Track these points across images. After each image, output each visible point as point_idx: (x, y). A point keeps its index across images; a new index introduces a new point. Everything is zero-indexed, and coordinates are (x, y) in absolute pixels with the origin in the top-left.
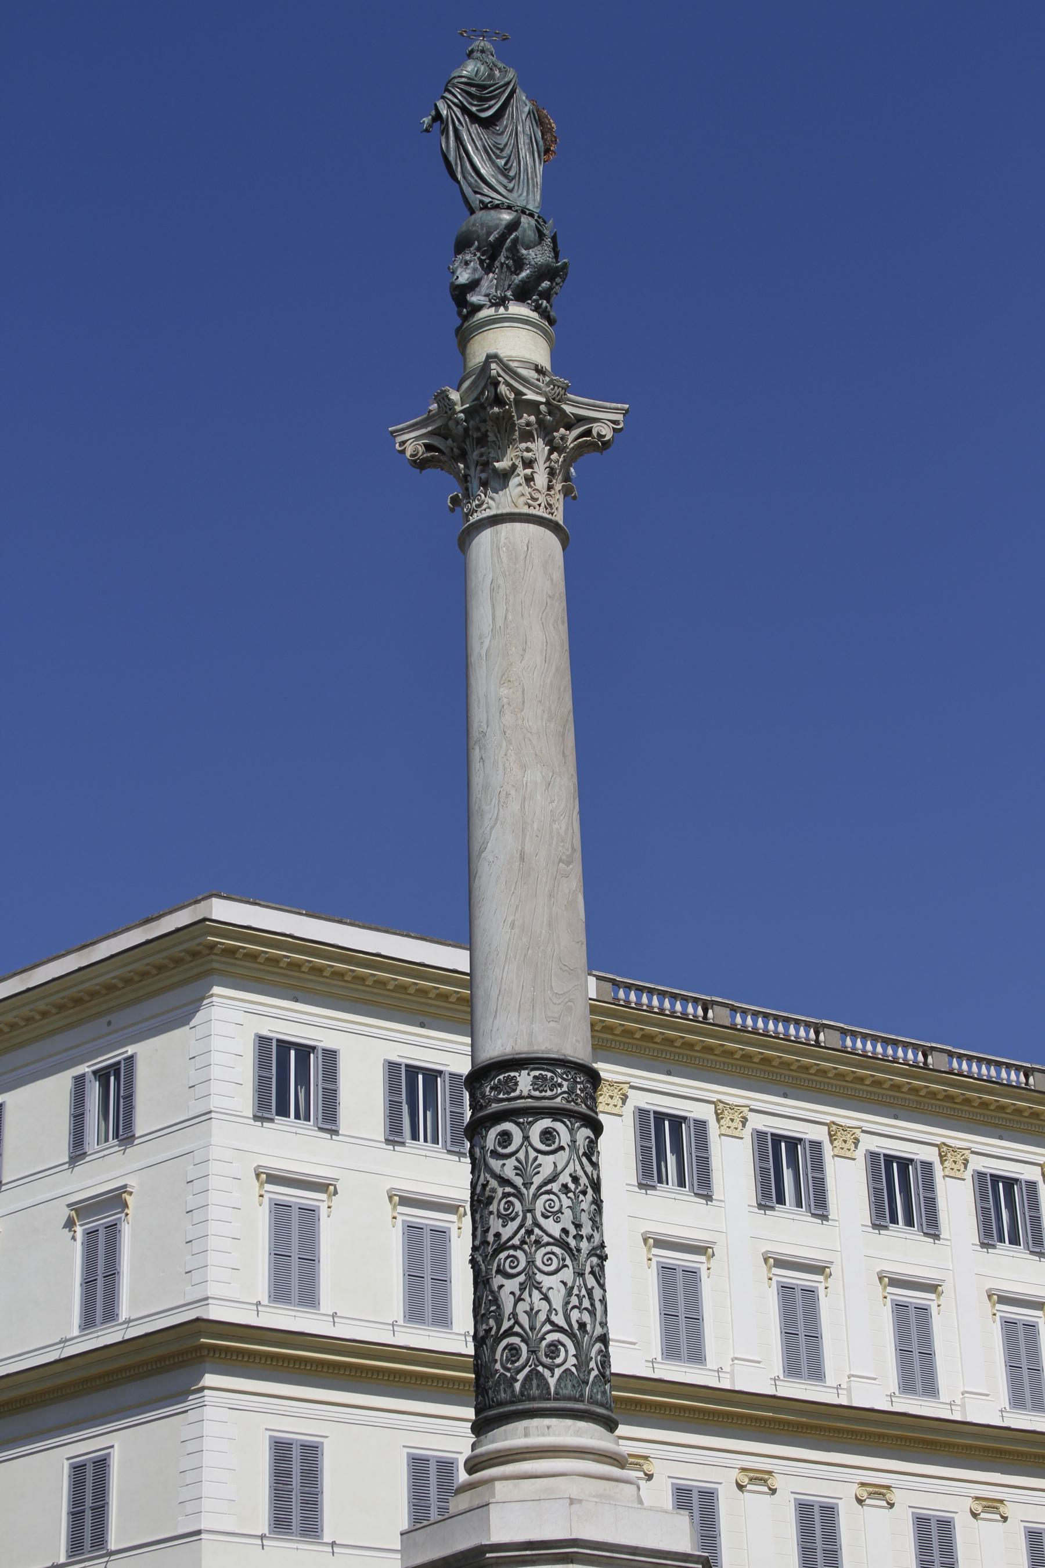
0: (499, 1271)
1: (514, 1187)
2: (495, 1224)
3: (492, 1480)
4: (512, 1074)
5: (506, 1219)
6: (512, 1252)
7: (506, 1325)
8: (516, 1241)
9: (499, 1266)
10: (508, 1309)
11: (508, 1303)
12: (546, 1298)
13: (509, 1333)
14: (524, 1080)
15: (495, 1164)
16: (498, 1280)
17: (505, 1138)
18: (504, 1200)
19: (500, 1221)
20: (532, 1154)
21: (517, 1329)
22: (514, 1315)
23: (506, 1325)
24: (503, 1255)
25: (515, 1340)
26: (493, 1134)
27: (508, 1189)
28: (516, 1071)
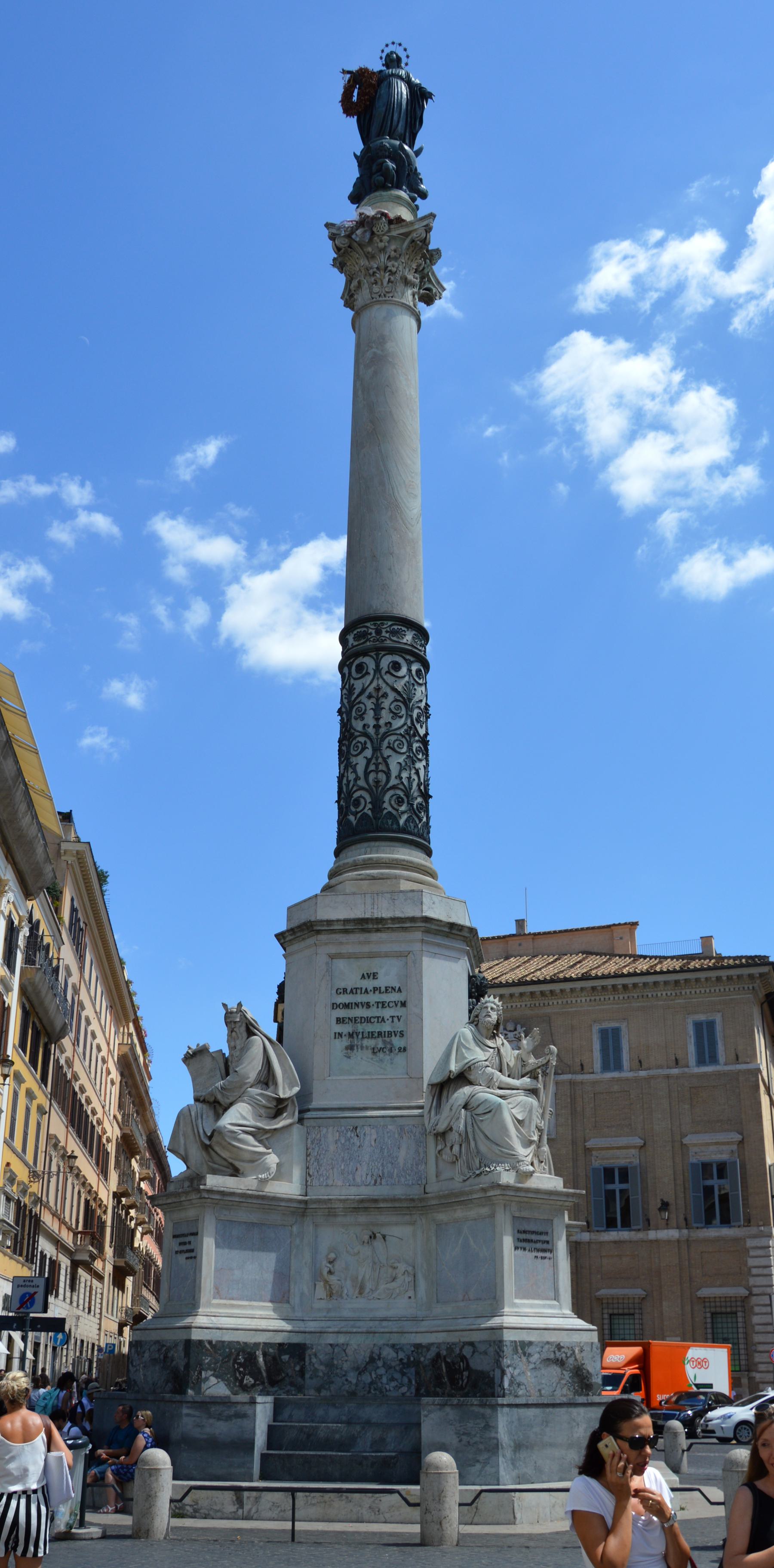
0: (389, 747)
1: (403, 698)
2: (386, 716)
3: (397, 877)
4: (403, 629)
5: (396, 715)
6: (400, 737)
7: (393, 781)
8: (402, 731)
9: (389, 743)
11: (394, 770)
12: (417, 773)
13: (394, 787)
15: (388, 678)
16: (387, 753)
17: (396, 666)
18: (395, 703)
19: (391, 715)
20: (412, 681)
21: (401, 786)
22: (399, 777)
23: (393, 781)
24: (392, 738)
25: (401, 794)
26: (386, 661)
27: (399, 698)
28: (408, 628)
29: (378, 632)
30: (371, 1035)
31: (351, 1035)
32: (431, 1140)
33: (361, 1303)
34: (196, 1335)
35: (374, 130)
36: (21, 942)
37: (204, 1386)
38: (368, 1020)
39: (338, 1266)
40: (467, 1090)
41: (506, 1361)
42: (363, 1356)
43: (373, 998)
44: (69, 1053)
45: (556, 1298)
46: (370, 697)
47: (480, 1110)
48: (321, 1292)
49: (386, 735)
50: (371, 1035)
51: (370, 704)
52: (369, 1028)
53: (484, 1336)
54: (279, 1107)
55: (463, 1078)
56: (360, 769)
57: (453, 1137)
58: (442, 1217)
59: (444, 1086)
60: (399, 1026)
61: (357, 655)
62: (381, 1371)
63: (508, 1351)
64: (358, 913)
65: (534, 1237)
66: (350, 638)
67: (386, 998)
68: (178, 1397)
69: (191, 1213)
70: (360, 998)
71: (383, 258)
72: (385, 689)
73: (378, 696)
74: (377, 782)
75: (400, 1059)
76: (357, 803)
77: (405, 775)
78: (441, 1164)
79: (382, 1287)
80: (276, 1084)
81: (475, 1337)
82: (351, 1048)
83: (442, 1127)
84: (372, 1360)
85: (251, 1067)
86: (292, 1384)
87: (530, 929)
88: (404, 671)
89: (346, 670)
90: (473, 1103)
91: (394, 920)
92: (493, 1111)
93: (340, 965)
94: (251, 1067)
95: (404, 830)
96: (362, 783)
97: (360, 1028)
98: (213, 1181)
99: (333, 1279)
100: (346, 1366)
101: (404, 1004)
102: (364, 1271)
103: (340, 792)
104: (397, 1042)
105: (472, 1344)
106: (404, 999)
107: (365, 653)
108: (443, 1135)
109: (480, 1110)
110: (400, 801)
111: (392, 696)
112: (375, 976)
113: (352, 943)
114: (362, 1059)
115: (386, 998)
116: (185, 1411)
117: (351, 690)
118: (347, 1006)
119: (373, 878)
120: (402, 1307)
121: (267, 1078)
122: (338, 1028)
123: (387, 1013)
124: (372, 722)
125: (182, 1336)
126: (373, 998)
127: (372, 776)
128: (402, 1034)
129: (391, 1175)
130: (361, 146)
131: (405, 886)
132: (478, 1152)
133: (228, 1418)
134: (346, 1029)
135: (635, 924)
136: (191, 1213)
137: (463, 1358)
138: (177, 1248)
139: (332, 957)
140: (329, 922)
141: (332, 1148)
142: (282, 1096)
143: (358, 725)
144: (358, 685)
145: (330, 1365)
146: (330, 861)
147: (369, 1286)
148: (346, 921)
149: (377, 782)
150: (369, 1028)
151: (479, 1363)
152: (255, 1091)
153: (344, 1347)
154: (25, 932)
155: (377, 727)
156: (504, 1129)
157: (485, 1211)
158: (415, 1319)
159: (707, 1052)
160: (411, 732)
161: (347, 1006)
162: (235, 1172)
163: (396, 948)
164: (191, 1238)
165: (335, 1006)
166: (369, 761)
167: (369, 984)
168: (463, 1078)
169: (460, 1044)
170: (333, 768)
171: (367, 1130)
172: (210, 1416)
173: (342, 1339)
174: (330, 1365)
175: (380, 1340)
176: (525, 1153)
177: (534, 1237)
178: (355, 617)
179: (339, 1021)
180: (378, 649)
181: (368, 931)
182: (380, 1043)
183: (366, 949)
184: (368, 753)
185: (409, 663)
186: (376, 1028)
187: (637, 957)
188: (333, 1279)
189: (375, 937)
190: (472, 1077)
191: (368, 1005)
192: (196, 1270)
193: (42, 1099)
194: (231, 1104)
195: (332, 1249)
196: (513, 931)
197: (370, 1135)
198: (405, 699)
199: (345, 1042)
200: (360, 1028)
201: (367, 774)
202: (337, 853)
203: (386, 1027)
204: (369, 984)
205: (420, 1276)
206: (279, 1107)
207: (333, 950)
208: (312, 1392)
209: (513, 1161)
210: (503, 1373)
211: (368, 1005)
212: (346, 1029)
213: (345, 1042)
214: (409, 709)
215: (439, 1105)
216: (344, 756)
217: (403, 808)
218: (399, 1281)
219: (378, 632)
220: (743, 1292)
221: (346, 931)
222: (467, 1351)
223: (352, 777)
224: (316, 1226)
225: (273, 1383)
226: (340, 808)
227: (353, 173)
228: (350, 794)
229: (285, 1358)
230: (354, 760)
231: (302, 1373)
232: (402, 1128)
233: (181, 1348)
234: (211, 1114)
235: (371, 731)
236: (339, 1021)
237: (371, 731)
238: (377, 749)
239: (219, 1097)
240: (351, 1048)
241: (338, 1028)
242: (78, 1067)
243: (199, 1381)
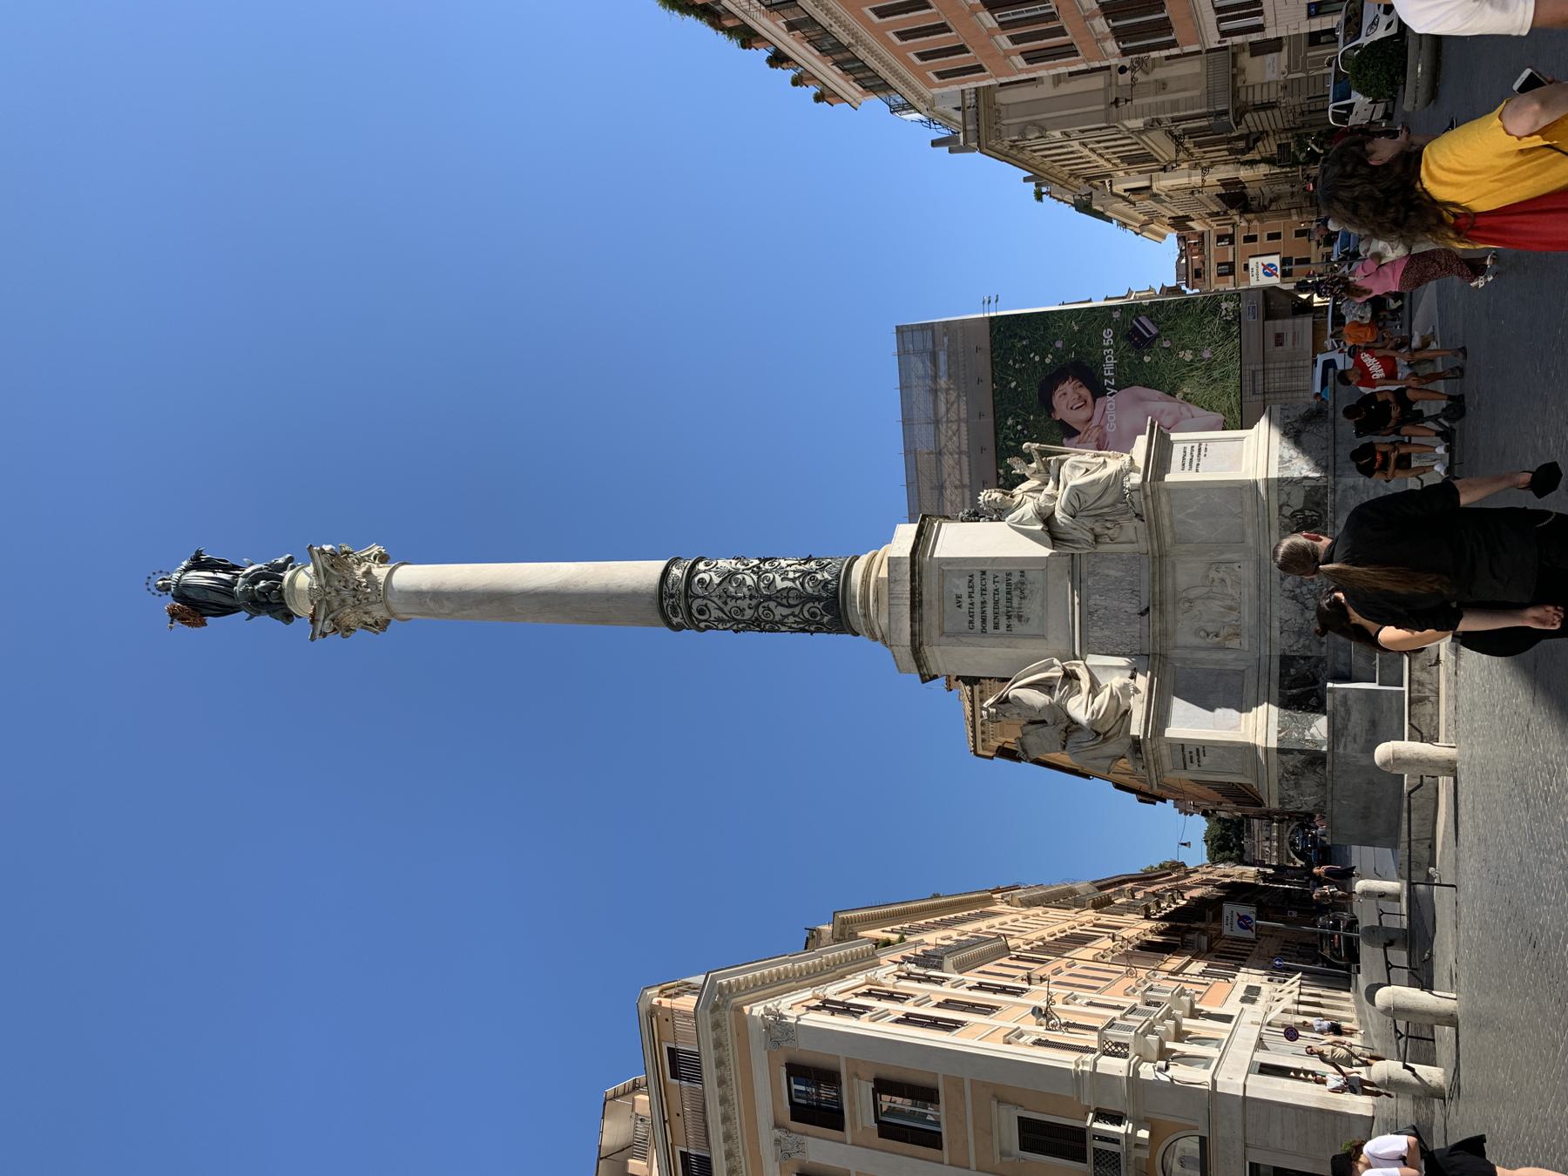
10: (790, 584)
11: (789, 584)
13: (802, 584)
14: (676, 572)
17: (701, 581)
22: (793, 580)
29: (672, 596)
30: (1009, 600)
31: (1009, 617)
32: (1101, 548)
33: (1245, 610)
34: (1273, 744)
35: (226, 601)
36: (921, 971)
37: (1319, 738)
38: (996, 603)
39: (1211, 628)
40: (1059, 515)
41: (1296, 475)
42: (1291, 604)
43: (977, 598)
44: (1020, 942)
45: (1241, 439)
46: (725, 603)
47: (1076, 504)
48: (1234, 643)
49: (757, 588)
50: (1009, 600)
51: (732, 603)
52: (1003, 602)
53: (1273, 497)
54: (1070, 677)
55: (1047, 519)
56: (785, 611)
57: (1098, 530)
58: (1168, 539)
60: (1002, 576)
61: (690, 614)
62: (1304, 589)
63: (1287, 474)
64: (906, 610)
65: (1188, 457)
66: (675, 620)
67: (977, 588)
68: (1329, 758)
69: (1165, 751)
70: (977, 610)
71: (345, 593)
72: (719, 591)
74: (797, 597)
75: (1030, 576)
76: (813, 615)
77: (791, 575)
78: (1122, 539)
79: (1230, 591)
80: (1051, 678)
81: (1274, 505)
82: (1020, 618)
83: (1090, 538)
84: (1295, 598)
86: (1316, 667)
88: (706, 576)
89: (702, 625)
90: (1071, 510)
91: (912, 580)
92: (1077, 491)
93: (948, 627)
94: (1038, 698)
95: (838, 576)
96: (797, 611)
97: (1002, 609)
98: (1136, 729)
99: (1223, 633)
100: (1300, 621)
101: (984, 573)
102: (1216, 606)
103: (803, 630)
104: (1015, 579)
105: (1280, 507)
106: (979, 571)
107: (689, 608)
108: (1097, 537)
109: (1076, 504)
110: (813, 579)
111: (725, 585)
112: (959, 597)
113: (931, 616)
114: (1032, 607)
115: (977, 588)
116: (1341, 750)
117: (720, 620)
118: (984, 621)
119: (877, 600)
120: (1247, 573)
121: (1045, 686)
122: (1003, 628)
123: (990, 586)
124: (748, 601)
125: (1274, 757)
126: (977, 598)
127: (792, 602)
128: (1009, 574)
129: (1132, 582)
130: (243, 615)
131: (884, 573)
132: (1113, 505)
133: (1348, 712)
134: (1003, 621)
136: (1165, 751)
137: (1293, 515)
138: (1195, 767)
139: (942, 633)
140: (913, 634)
141: (1107, 633)
142: (1061, 674)
143: (749, 613)
144: (716, 613)
145: (1300, 633)
146: (864, 640)
147: (1229, 603)
148: (912, 619)
149: (797, 597)
150: (1003, 602)
151: (1297, 501)
152: (1057, 695)
153: (1283, 622)
154: (912, 967)
155: (751, 597)
156: (1093, 483)
157: (1164, 499)
158: (1259, 563)
161: (984, 621)
162: (1127, 713)
163: (935, 580)
164: (1187, 751)
165: (984, 631)
166: (780, 604)
167: (966, 601)
168: (1047, 519)
169: (1019, 522)
170: (783, 639)
171: (1091, 602)
172: (1345, 727)
173: (1276, 624)
174: (1300, 633)
175: (1277, 591)
176: (1114, 465)
177: (1188, 457)
178: (658, 616)
179: (996, 627)
180: (686, 596)
181: (921, 602)
182: (1016, 593)
183: (936, 603)
184: (772, 605)
185: (699, 572)
186: (1002, 597)
188: (1223, 633)
189: (925, 597)
190: (1049, 512)
191: (984, 603)
192: (1215, 745)
193: (1062, 963)
194: (1069, 716)
195: (1196, 633)
197: (1096, 600)
199: (1014, 622)
200: (1002, 609)
201: (790, 606)
202: (856, 634)
203: (1003, 587)
204: (966, 601)
205: (1221, 558)
207: (935, 633)
208: (1324, 649)
209: (1120, 475)
210: (1306, 478)
211: (984, 603)
212: (1003, 621)
213: (1014, 622)
214: (737, 572)
215: (1072, 541)
216: (773, 627)
217: (819, 576)
218: (1225, 576)
219: (672, 596)
221: (921, 620)
222: (1287, 511)
223: (791, 619)
224: (1175, 647)
225: (1315, 682)
226: (818, 630)
227: (265, 621)
228: (806, 621)
229: (1293, 671)
230: (778, 618)
231: (1306, 658)
232: (1089, 573)
233: (1284, 758)
234: (1076, 735)
235: (754, 602)
236: (996, 627)
237: (754, 602)
238: (769, 598)
239: (1062, 726)
240: (1020, 618)
241: (1003, 628)
242: (1032, 937)
243: (1314, 742)
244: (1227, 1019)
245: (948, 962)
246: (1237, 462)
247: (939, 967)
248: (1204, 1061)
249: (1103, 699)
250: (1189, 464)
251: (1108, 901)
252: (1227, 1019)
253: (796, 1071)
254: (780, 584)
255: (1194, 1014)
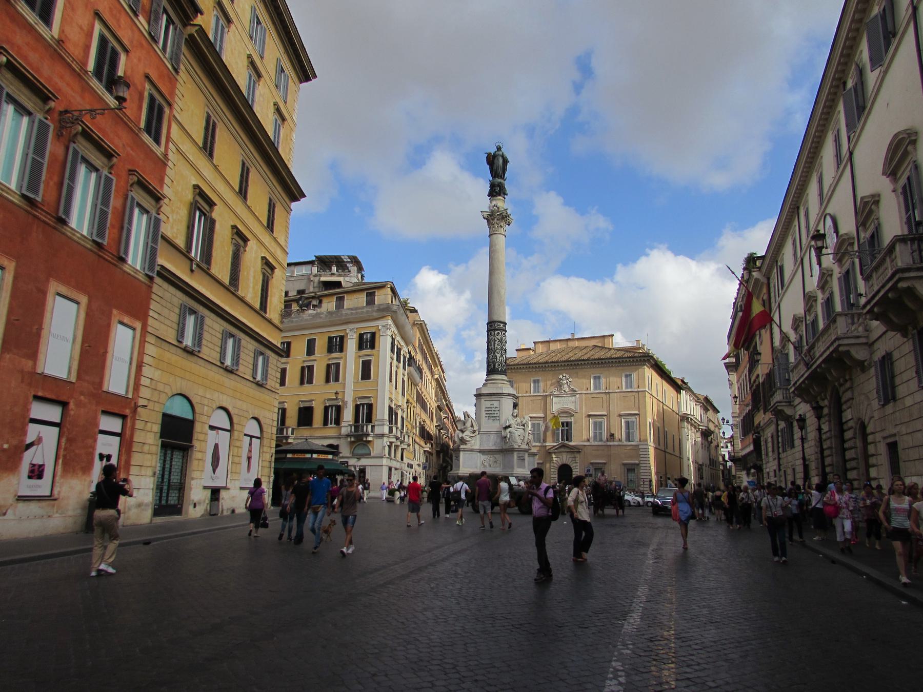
54: (474, 432)
55: (509, 426)
59: (506, 428)
73: (495, 341)
85: (468, 424)
87: (577, 336)
113: (488, 398)
114: (491, 421)
121: (472, 426)
135: (612, 336)
159: (629, 385)
160: (502, 348)
168: (509, 426)
187: (610, 349)
193: (414, 404)
196: (570, 337)
197: (492, 437)
198: (501, 341)
206: (474, 432)
220: (637, 462)
244: (402, 459)
245: (412, 369)
246: (519, 467)
247: (409, 365)
248: (390, 454)
249: (469, 439)
250: (519, 458)
251: (441, 410)
252: (402, 459)
253: (373, 335)
254: (498, 356)
255: (403, 449)
